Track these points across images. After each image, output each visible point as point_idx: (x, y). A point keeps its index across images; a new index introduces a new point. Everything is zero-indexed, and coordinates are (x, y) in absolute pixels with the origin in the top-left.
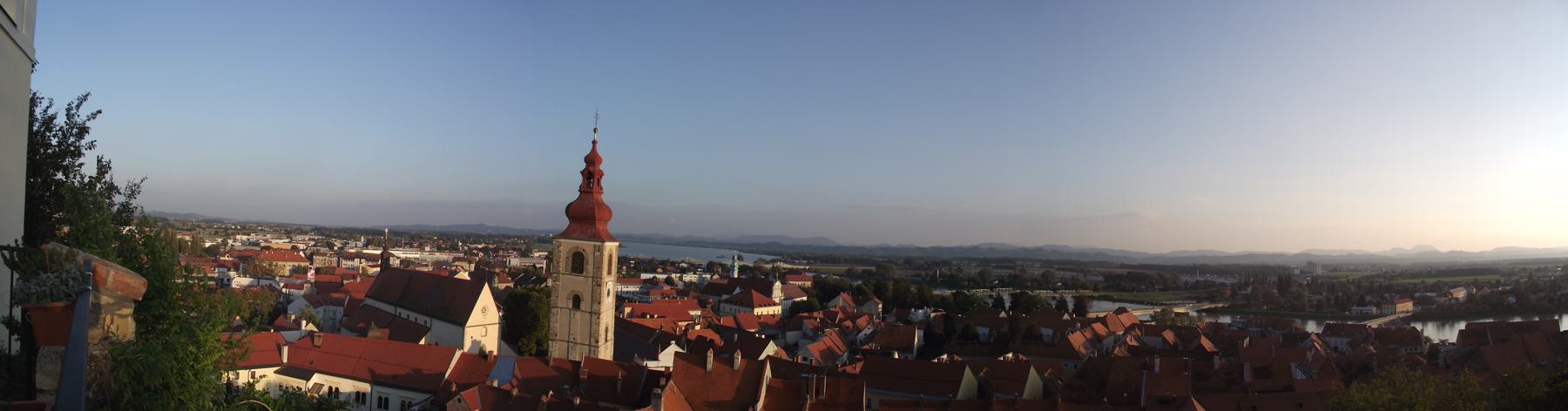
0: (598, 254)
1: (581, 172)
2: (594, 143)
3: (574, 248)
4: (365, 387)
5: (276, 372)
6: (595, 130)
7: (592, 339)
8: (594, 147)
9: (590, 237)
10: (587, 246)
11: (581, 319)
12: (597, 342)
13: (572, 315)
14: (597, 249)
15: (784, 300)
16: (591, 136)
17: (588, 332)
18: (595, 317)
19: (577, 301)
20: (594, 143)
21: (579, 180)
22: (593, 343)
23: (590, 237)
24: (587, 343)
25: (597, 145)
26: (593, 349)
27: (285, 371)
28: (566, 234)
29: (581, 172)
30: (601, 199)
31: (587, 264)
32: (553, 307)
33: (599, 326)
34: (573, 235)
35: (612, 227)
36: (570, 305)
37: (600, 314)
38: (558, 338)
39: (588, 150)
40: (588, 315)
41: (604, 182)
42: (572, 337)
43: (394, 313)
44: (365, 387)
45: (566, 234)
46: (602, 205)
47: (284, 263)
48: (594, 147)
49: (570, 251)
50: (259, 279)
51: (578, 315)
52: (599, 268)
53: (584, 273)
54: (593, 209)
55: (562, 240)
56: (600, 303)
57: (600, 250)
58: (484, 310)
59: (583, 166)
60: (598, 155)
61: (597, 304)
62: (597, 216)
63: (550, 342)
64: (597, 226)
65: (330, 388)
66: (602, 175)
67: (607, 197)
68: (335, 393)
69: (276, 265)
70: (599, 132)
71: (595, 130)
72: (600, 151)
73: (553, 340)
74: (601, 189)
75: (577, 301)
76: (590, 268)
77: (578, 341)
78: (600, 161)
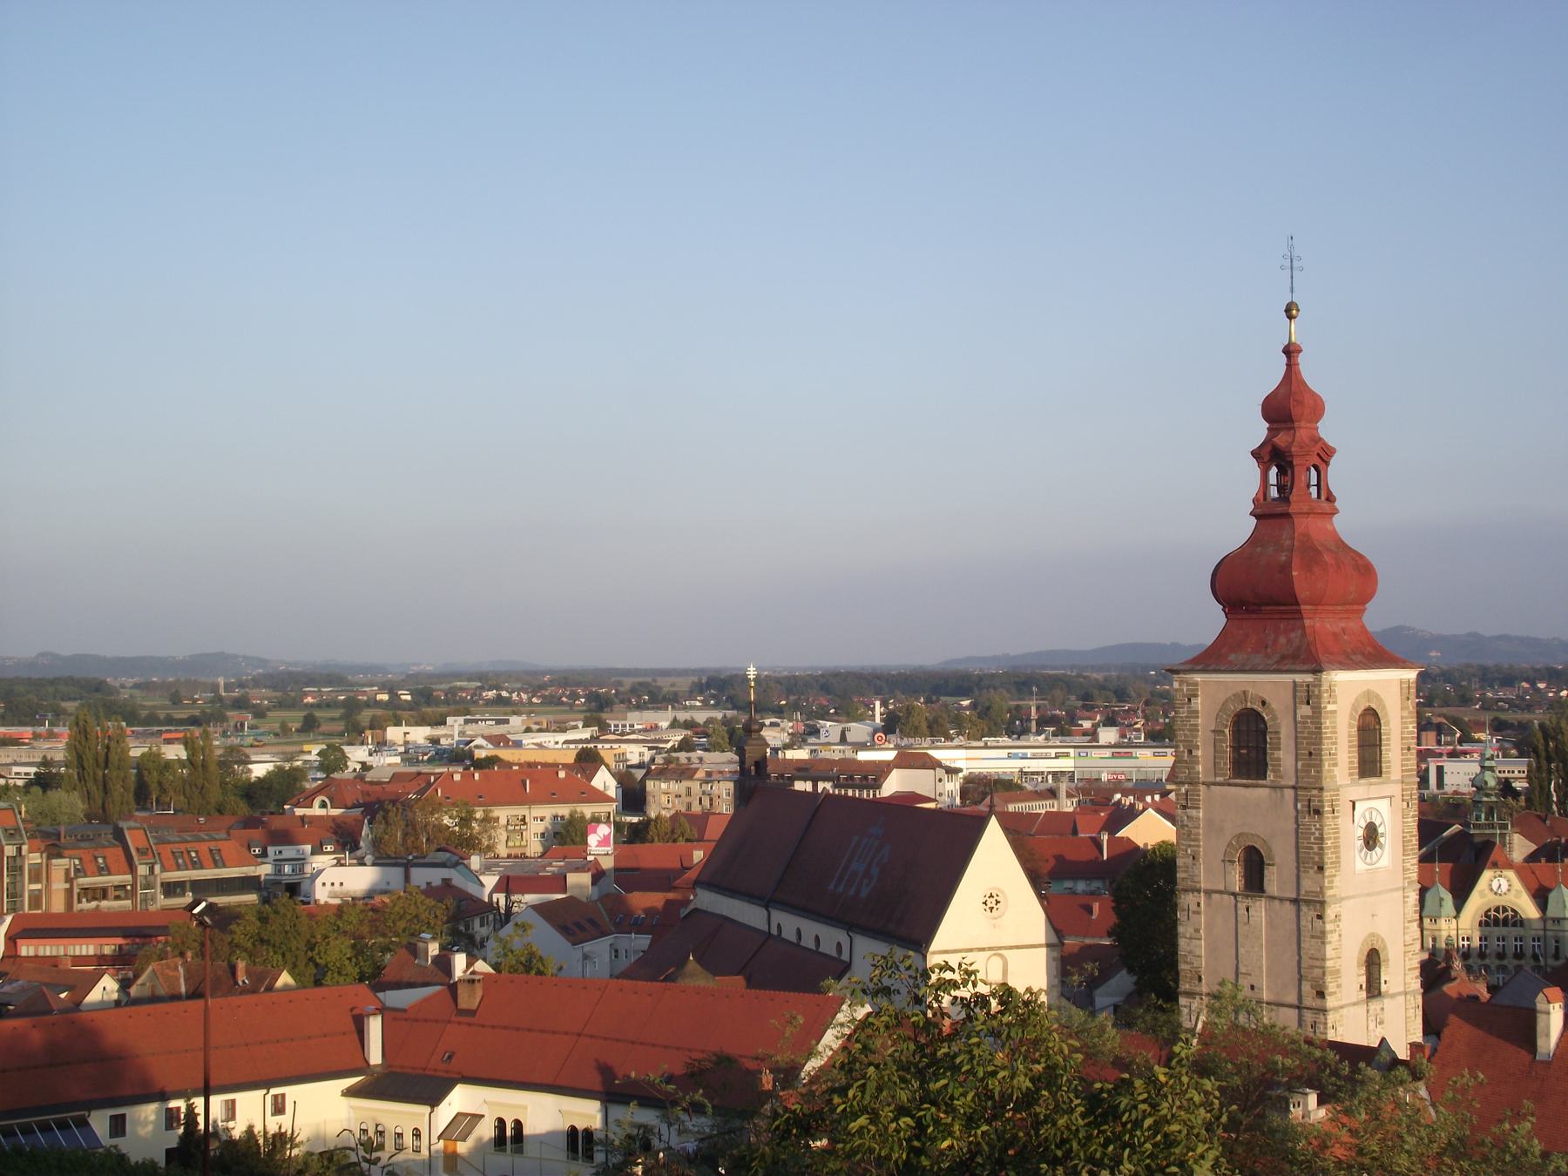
0: (1305, 710)
1: (1254, 453)
2: (1290, 351)
4: (587, 1113)
5: (350, 1093)
6: (1290, 310)
7: (1306, 987)
8: (1291, 366)
9: (1283, 658)
11: (1271, 924)
12: (1321, 994)
13: (1242, 911)
14: (1302, 694)
16: (1284, 332)
17: (1295, 963)
18: (1308, 913)
19: (1254, 865)
20: (1290, 351)
21: (1247, 479)
22: (1309, 1000)
23: (1283, 658)
24: (1292, 998)
25: (1302, 360)
26: (1309, 1016)
27: (379, 1087)
28: (1211, 659)
29: (1254, 453)
30: (1334, 533)
32: (1186, 891)
33: (1323, 943)
34: (1232, 657)
35: (1377, 617)
36: (1236, 879)
37: (1323, 903)
39: (1272, 378)
40: (1288, 906)
41: (1336, 475)
42: (1244, 982)
43: (764, 927)
44: (587, 1113)
45: (1211, 659)
46: (1312, 554)
47: (520, 811)
48: (1291, 366)
50: (407, 866)
51: (1260, 910)
53: (1270, 776)
54: (1286, 568)
55: (1198, 678)
56: (1321, 869)
57: (1310, 697)
58: (992, 902)
59: (1258, 431)
62: (1302, 590)
64: (1307, 622)
65: (501, 1123)
66: (1325, 454)
68: (510, 1138)
69: (487, 820)
71: (1290, 310)
73: (1190, 994)
74: (1330, 498)
75: (1254, 865)
76: (1284, 757)
77: (1265, 996)
78: (1317, 409)
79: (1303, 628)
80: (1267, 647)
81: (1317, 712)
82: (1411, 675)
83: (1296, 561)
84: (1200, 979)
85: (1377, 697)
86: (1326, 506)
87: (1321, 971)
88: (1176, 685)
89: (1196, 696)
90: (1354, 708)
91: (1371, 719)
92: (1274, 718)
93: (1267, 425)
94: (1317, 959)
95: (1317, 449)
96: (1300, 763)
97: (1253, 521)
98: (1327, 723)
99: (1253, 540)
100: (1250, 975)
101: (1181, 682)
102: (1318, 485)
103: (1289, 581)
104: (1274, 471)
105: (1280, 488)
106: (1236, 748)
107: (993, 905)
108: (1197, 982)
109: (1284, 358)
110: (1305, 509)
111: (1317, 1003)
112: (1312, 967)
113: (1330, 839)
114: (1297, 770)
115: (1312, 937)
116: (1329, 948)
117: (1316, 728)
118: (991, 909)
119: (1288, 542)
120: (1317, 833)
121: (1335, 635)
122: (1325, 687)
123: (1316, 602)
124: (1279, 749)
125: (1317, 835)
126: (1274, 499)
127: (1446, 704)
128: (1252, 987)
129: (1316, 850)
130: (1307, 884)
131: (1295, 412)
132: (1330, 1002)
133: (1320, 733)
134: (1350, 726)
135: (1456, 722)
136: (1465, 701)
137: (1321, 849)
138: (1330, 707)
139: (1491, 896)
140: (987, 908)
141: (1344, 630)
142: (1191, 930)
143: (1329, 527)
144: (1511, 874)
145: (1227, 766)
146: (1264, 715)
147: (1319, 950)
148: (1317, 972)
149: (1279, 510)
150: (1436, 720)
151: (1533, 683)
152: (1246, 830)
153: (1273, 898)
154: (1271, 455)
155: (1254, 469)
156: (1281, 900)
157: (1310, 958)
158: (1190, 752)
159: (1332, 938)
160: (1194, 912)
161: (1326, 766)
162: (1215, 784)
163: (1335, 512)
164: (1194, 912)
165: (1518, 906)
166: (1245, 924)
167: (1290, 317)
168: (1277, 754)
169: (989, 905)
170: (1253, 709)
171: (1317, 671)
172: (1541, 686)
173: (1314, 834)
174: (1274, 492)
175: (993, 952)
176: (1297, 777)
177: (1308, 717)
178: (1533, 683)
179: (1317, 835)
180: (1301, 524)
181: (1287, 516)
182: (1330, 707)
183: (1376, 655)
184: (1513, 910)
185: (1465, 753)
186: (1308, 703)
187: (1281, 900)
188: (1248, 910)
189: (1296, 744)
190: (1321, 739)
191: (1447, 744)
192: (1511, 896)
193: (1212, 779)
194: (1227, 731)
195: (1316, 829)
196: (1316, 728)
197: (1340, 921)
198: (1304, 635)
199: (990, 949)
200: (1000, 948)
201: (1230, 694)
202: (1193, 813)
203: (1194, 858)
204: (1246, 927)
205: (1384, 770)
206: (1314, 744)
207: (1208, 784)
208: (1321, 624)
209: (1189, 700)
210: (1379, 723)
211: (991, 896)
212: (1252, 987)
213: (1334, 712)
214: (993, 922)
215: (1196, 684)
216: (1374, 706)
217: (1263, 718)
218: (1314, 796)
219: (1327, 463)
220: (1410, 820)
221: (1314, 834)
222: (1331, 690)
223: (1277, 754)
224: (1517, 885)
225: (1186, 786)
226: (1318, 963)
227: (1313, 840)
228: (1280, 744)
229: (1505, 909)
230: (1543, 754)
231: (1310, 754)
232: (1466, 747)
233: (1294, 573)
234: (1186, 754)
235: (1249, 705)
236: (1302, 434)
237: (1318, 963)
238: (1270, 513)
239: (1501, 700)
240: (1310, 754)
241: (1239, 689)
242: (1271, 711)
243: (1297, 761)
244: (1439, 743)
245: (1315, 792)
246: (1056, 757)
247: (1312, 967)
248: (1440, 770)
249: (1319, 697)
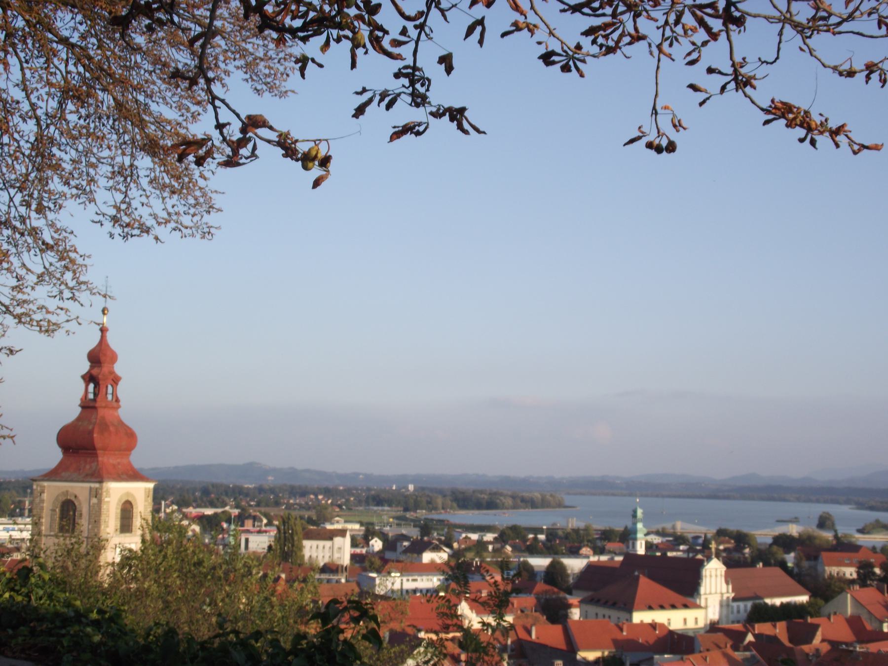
0: (94, 500)
1: (83, 377)
2: (103, 330)
3: (63, 493)
9: (87, 475)
10: (79, 489)
14: (94, 493)
15: (735, 599)
20: (103, 330)
28: (53, 475)
29: (83, 377)
34: (63, 474)
35: (138, 459)
39: (93, 341)
45: (53, 475)
46: (104, 426)
49: (57, 499)
52: (96, 519)
54: (91, 432)
55: (46, 484)
57: (97, 494)
59: (85, 366)
60: (108, 346)
62: (98, 443)
64: (100, 459)
66: (116, 380)
67: (128, 413)
70: (111, 313)
72: (113, 341)
74: (117, 400)
76: (84, 524)
78: (114, 358)
79: (98, 461)
80: (80, 470)
81: (100, 502)
82: (151, 485)
83: (96, 430)
85: (132, 495)
86: (115, 404)
88: (35, 487)
89: (43, 492)
90: (120, 500)
91: (128, 506)
92: (80, 504)
95: (112, 377)
96: (90, 526)
97: (80, 409)
98: (104, 507)
99: (79, 419)
101: (37, 486)
102: (113, 394)
103: (92, 439)
105: (95, 394)
106: (61, 518)
109: (99, 333)
110: (104, 405)
114: (88, 529)
119: (94, 420)
121: (114, 466)
122: (104, 490)
123: (105, 449)
126: (91, 400)
127: (267, 505)
131: (102, 359)
134: (117, 508)
135: (266, 515)
136: (277, 504)
138: (107, 499)
141: (119, 464)
143: (116, 414)
145: (56, 527)
149: (92, 404)
150: (253, 514)
151: (316, 496)
154: (89, 378)
155: (82, 384)
161: (102, 527)
162: (50, 535)
163: (119, 407)
167: (104, 313)
171: (101, 482)
172: (320, 497)
174: (91, 396)
176: (88, 532)
178: (316, 496)
180: (101, 412)
181: (95, 408)
182: (107, 499)
183: (135, 476)
185: (266, 532)
189: (89, 516)
191: (258, 526)
193: (48, 533)
194: (58, 510)
198: (98, 465)
207: (46, 536)
208: (106, 460)
210: (132, 507)
213: (108, 502)
215: (44, 487)
216: (130, 499)
217: (74, 504)
222: (108, 491)
223: (79, 521)
230: (282, 531)
232: (268, 528)
233: (95, 435)
235: (69, 497)
236: (105, 369)
238: (88, 406)
239: (296, 504)
241: (64, 490)
243: (89, 524)
244: (254, 526)
248: (247, 541)
249: (101, 494)
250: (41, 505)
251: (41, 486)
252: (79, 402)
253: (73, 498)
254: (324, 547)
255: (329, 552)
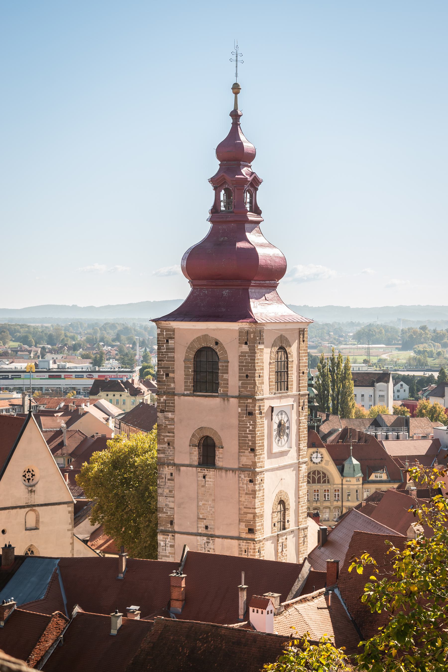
0: (245, 348)
6: (236, 88)
12: (251, 531)
25: (241, 120)
31: (226, 371)
33: (254, 498)
38: (176, 528)
53: (221, 390)
56: (253, 450)
61: (247, 452)
63: (160, 537)
73: (165, 532)
84: (172, 523)
87: (252, 515)
93: (220, 163)
94: (250, 508)
97: (209, 225)
98: (258, 356)
100: (205, 519)
104: (223, 192)
107: (30, 477)
108: (169, 526)
109: (230, 120)
111: (250, 536)
112: (246, 513)
113: (259, 430)
115: (247, 494)
116: (257, 500)
117: (251, 360)
118: (29, 479)
120: (251, 427)
124: (227, 373)
125: (251, 428)
128: (207, 527)
129: (250, 438)
130: (246, 460)
132: (258, 536)
133: (254, 363)
137: (254, 437)
139: (312, 465)
140: (26, 479)
142: (167, 491)
144: (324, 451)
146: (217, 351)
147: (251, 502)
148: (250, 516)
152: (203, 425)
153: (221, 469)
156: (227, 470)
157: (245, 508)
158: (167, 375)
159: (259, 494)
160: (169, 480)
162: (184, 395)
164: (169, 480)
165: (328, 470)
166: (203, 486)
168: (225, 376)
169: (27, 477)
170: (210, 348)
173: (249, 427)
175: (30, 509)
177: (246, 353)
179: (251, 428)
184: (323, 473)
186: (246, 343)
187: (227, 470)
188: (204, 477)
190: (254, 366)
192: (323, 464)
195: (250, 425)
196: (251, 360)
197: (263, 483)
199: (28, 506)
200: (34, 506)
201: (195, 337)
202: (170, 415)
203: (169, 444)
204: (203, 489)
205: (289, 386)
206: (250, 370)
209: (167, 341)
211: (29, 471)
212: (207, 527)
214: (30, 489)
215: (173, 330)
217: (216, 353)
218: (250, 403)
219: (256, 189)
220: (303, 418)
221: (249, 427)
224: (327, 457)
225: (164, 397)
226: (250, 511)
227: (248, 432)
228: (227, 370)
229: (319, 473)
231: (247, 376)
234: (165, 377)
237: (250, 511)
240: (247, 376)
242: (223, 348)
245: (250, 401)
246: (12, 379)
247: (246, 513)
250: (170, 355)
251: (168, 330)
252: (208, 215)
253: (212, 345)
254: (363, 396)
255: (370, 400)
